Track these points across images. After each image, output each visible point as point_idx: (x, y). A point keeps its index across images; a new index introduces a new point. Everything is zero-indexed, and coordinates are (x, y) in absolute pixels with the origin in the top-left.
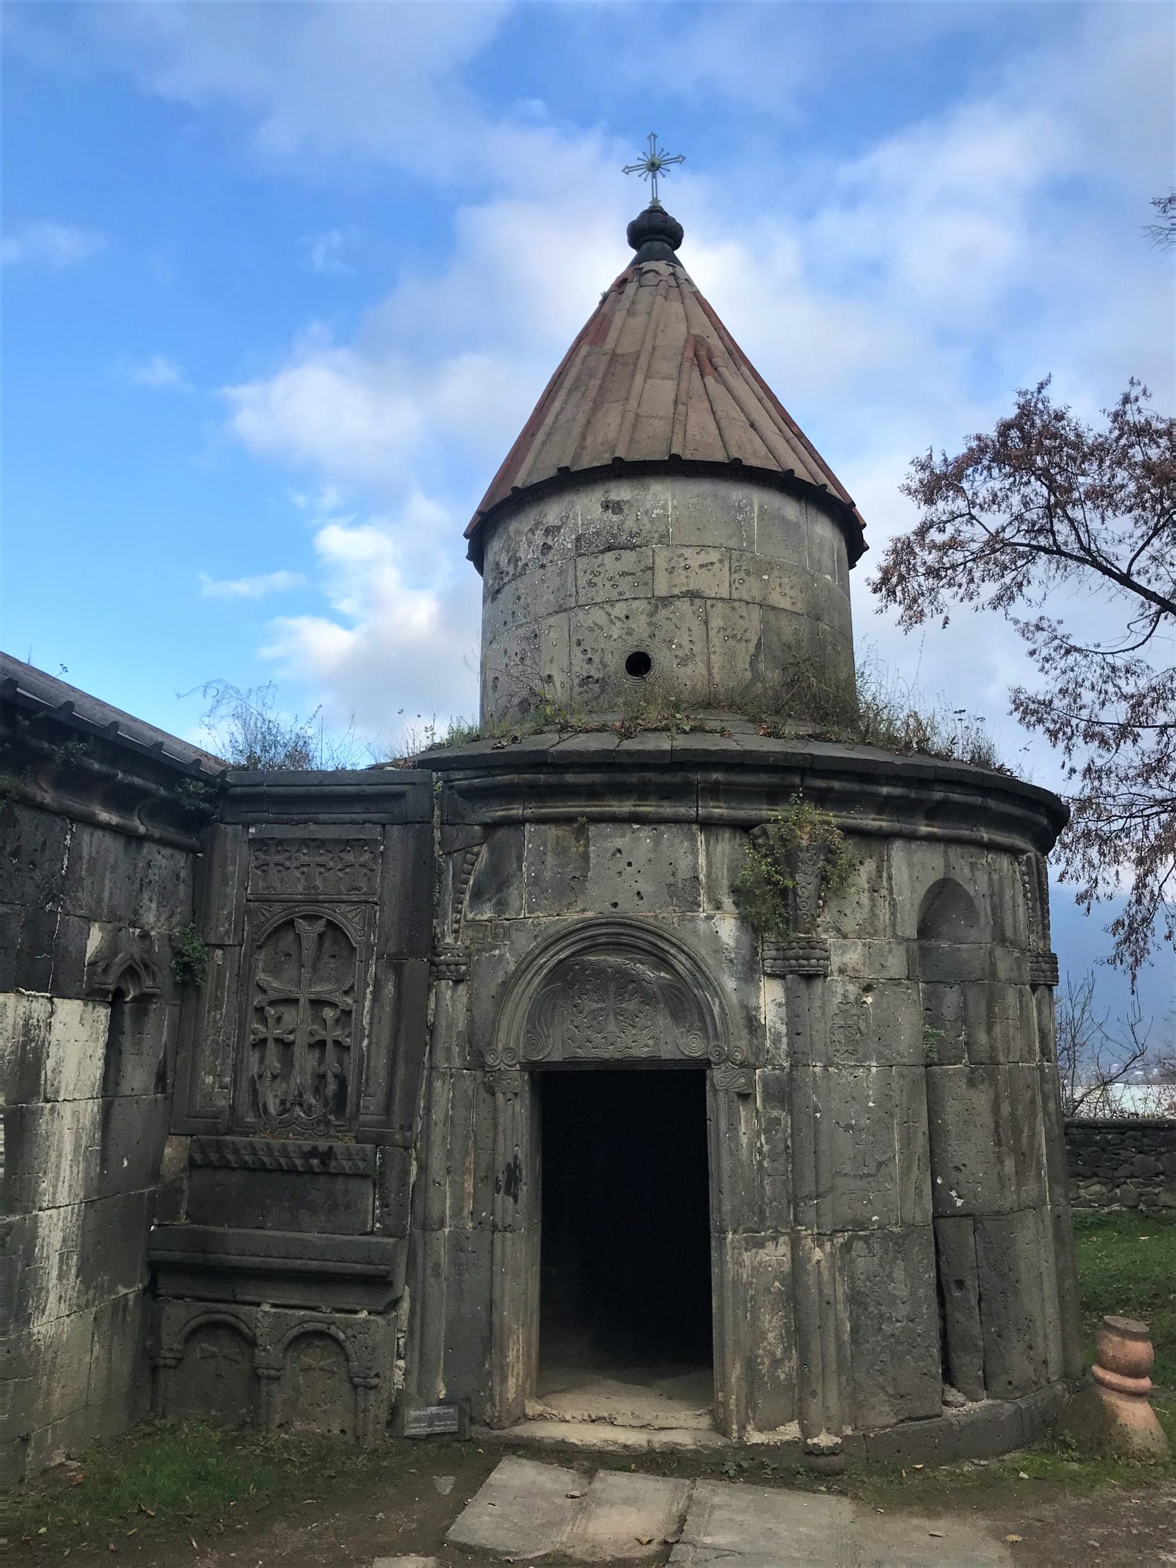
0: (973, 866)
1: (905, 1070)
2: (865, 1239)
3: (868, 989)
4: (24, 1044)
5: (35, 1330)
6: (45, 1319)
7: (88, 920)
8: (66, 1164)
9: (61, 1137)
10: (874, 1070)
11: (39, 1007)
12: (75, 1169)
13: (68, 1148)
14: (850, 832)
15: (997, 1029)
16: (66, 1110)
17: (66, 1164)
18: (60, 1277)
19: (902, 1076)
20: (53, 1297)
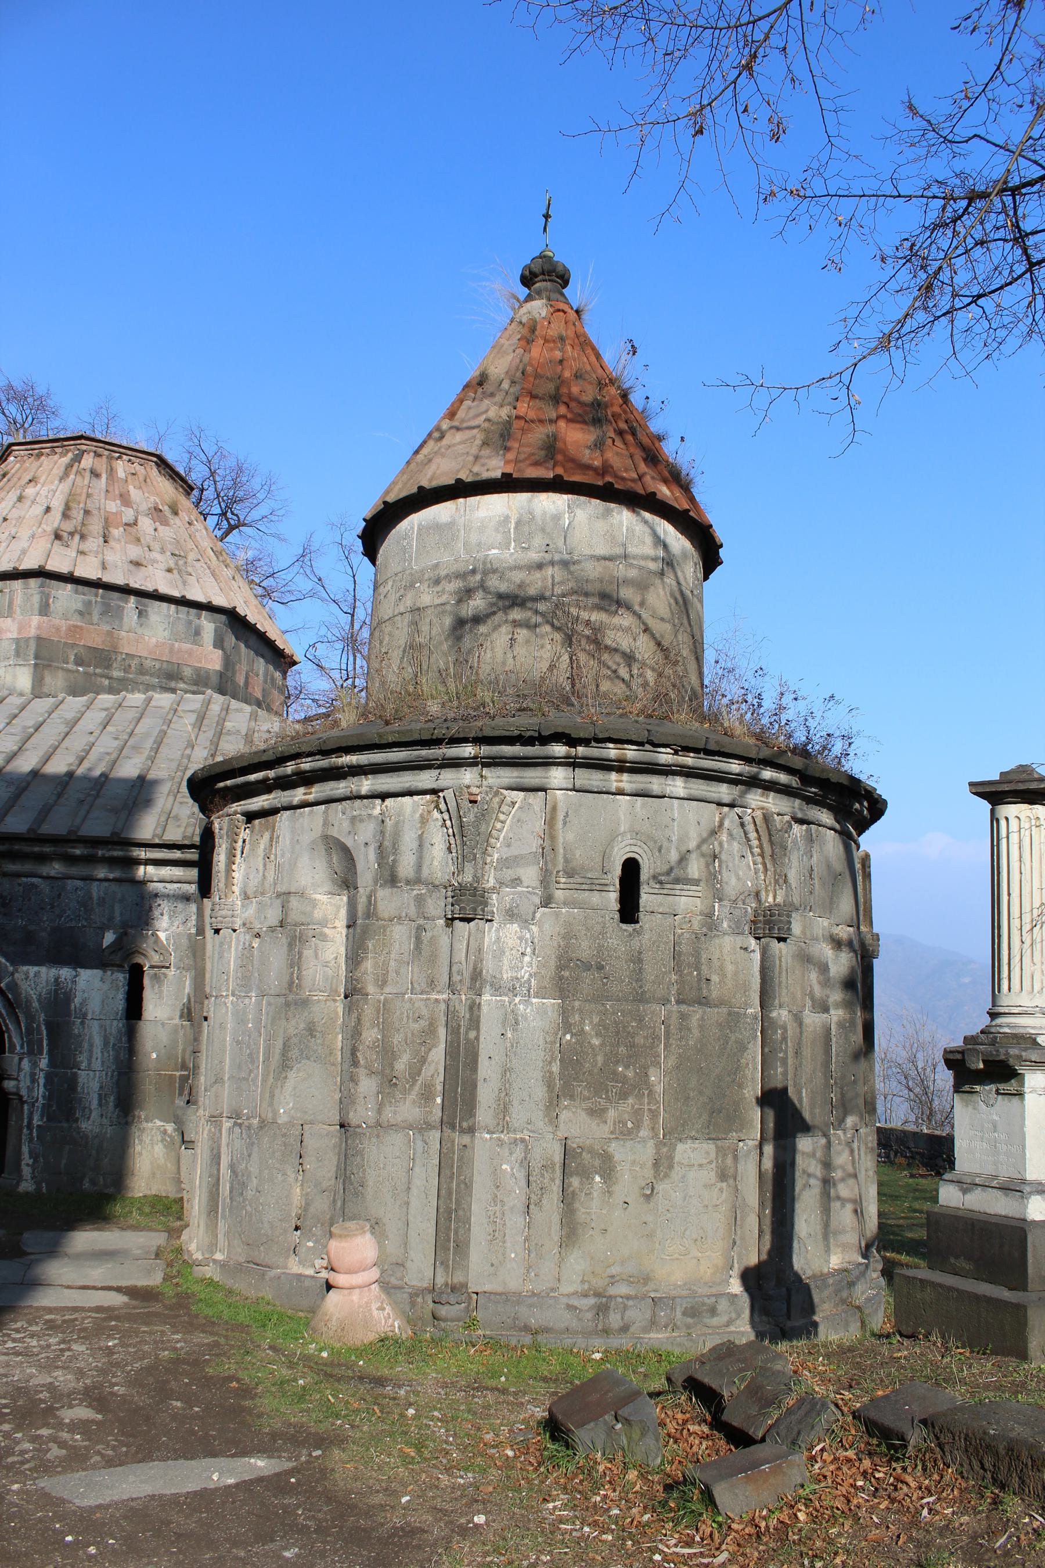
0: (353, 820)
1: (272, 1000)
2: (240, 1125)
3: (258, 936)
4: (56, 991)
5: (83, 1126)
6: (90, 1122)
7: (103, 929)
8: (97, 1051)
9: (91, 1037)
10: (253, 999)
11: (65, 973)
12: (106, 1055)
13: (98, 1041)
14: (250, 817)
15: (368, 965)
16: (95, 1025)
17: (97, 1051)
18: (100, 1105)
19: (269, 1004)
20: (95, 1115)
